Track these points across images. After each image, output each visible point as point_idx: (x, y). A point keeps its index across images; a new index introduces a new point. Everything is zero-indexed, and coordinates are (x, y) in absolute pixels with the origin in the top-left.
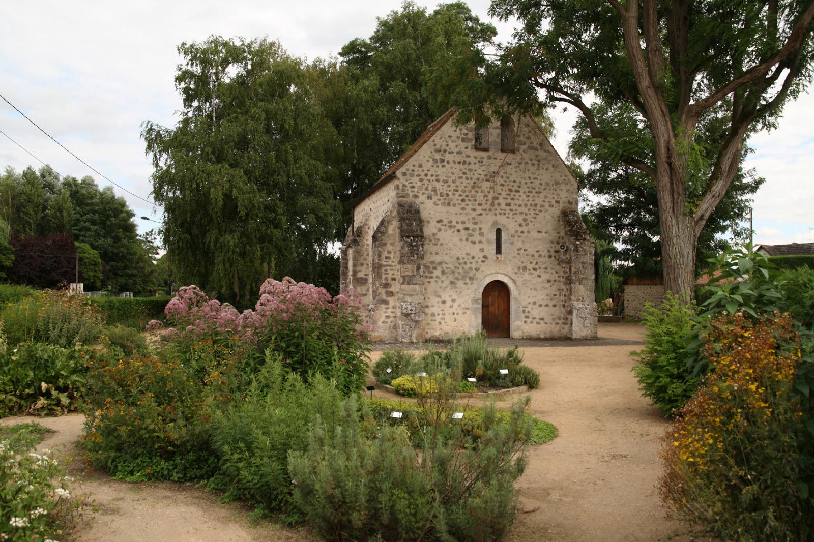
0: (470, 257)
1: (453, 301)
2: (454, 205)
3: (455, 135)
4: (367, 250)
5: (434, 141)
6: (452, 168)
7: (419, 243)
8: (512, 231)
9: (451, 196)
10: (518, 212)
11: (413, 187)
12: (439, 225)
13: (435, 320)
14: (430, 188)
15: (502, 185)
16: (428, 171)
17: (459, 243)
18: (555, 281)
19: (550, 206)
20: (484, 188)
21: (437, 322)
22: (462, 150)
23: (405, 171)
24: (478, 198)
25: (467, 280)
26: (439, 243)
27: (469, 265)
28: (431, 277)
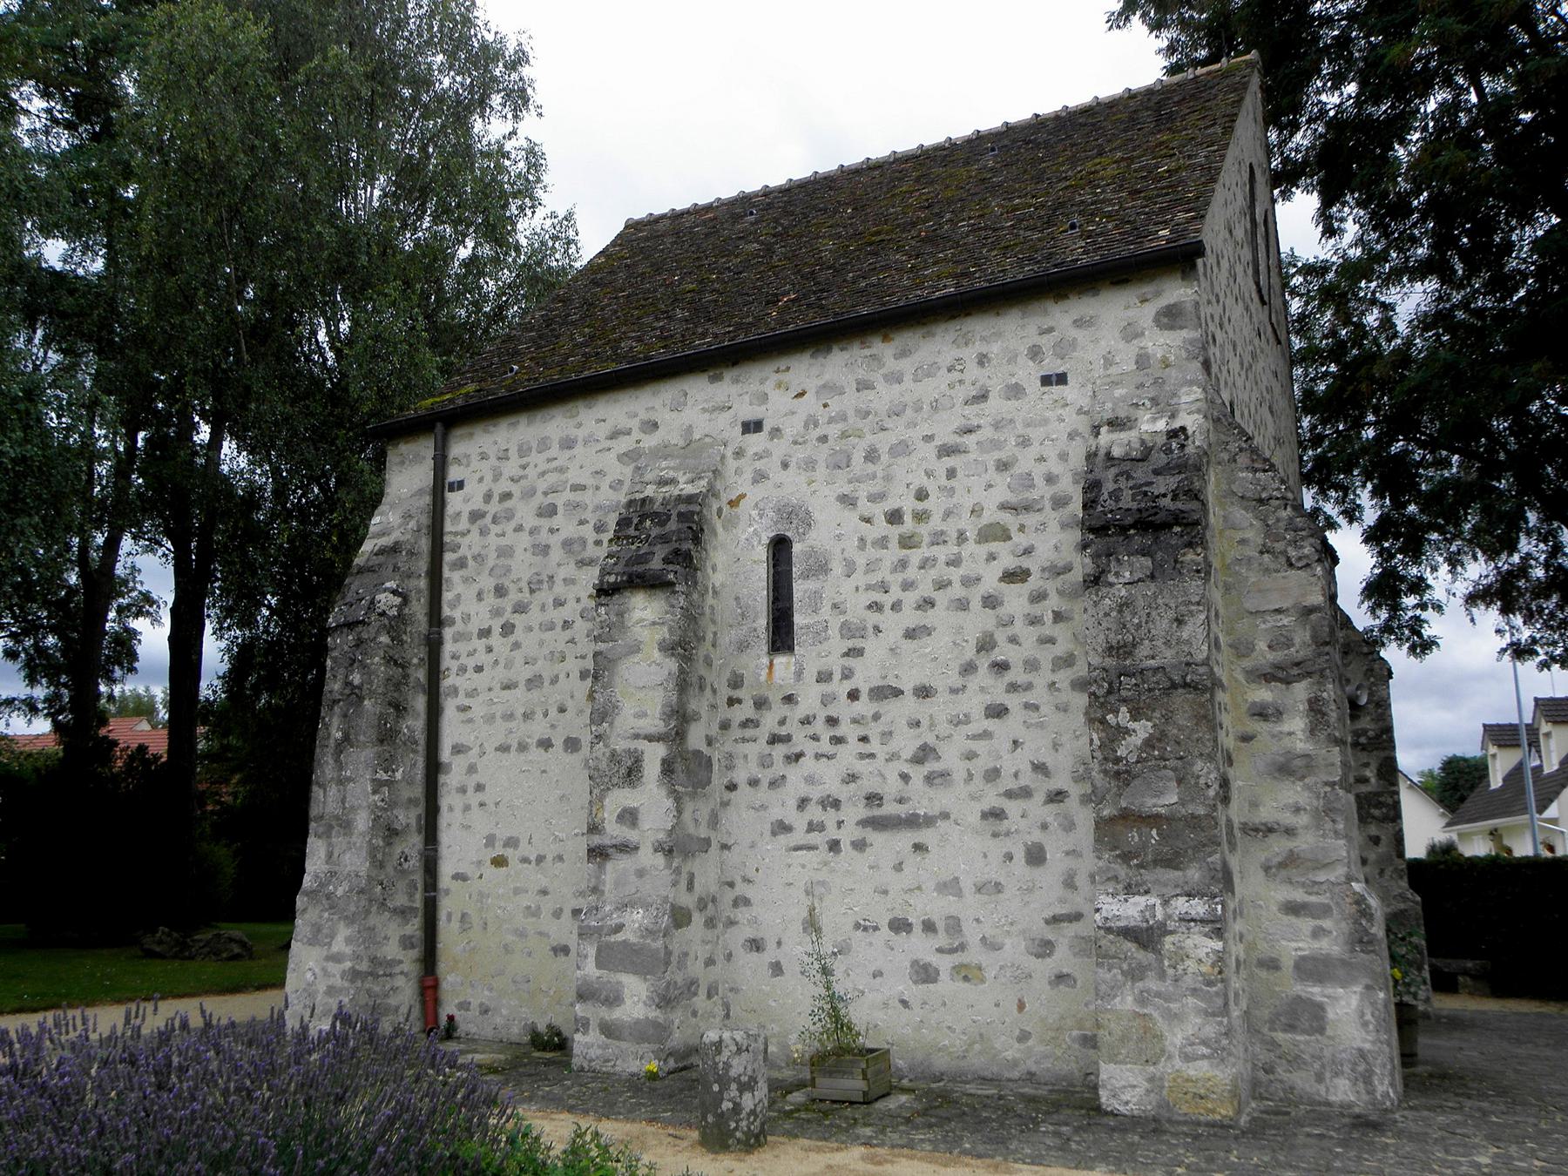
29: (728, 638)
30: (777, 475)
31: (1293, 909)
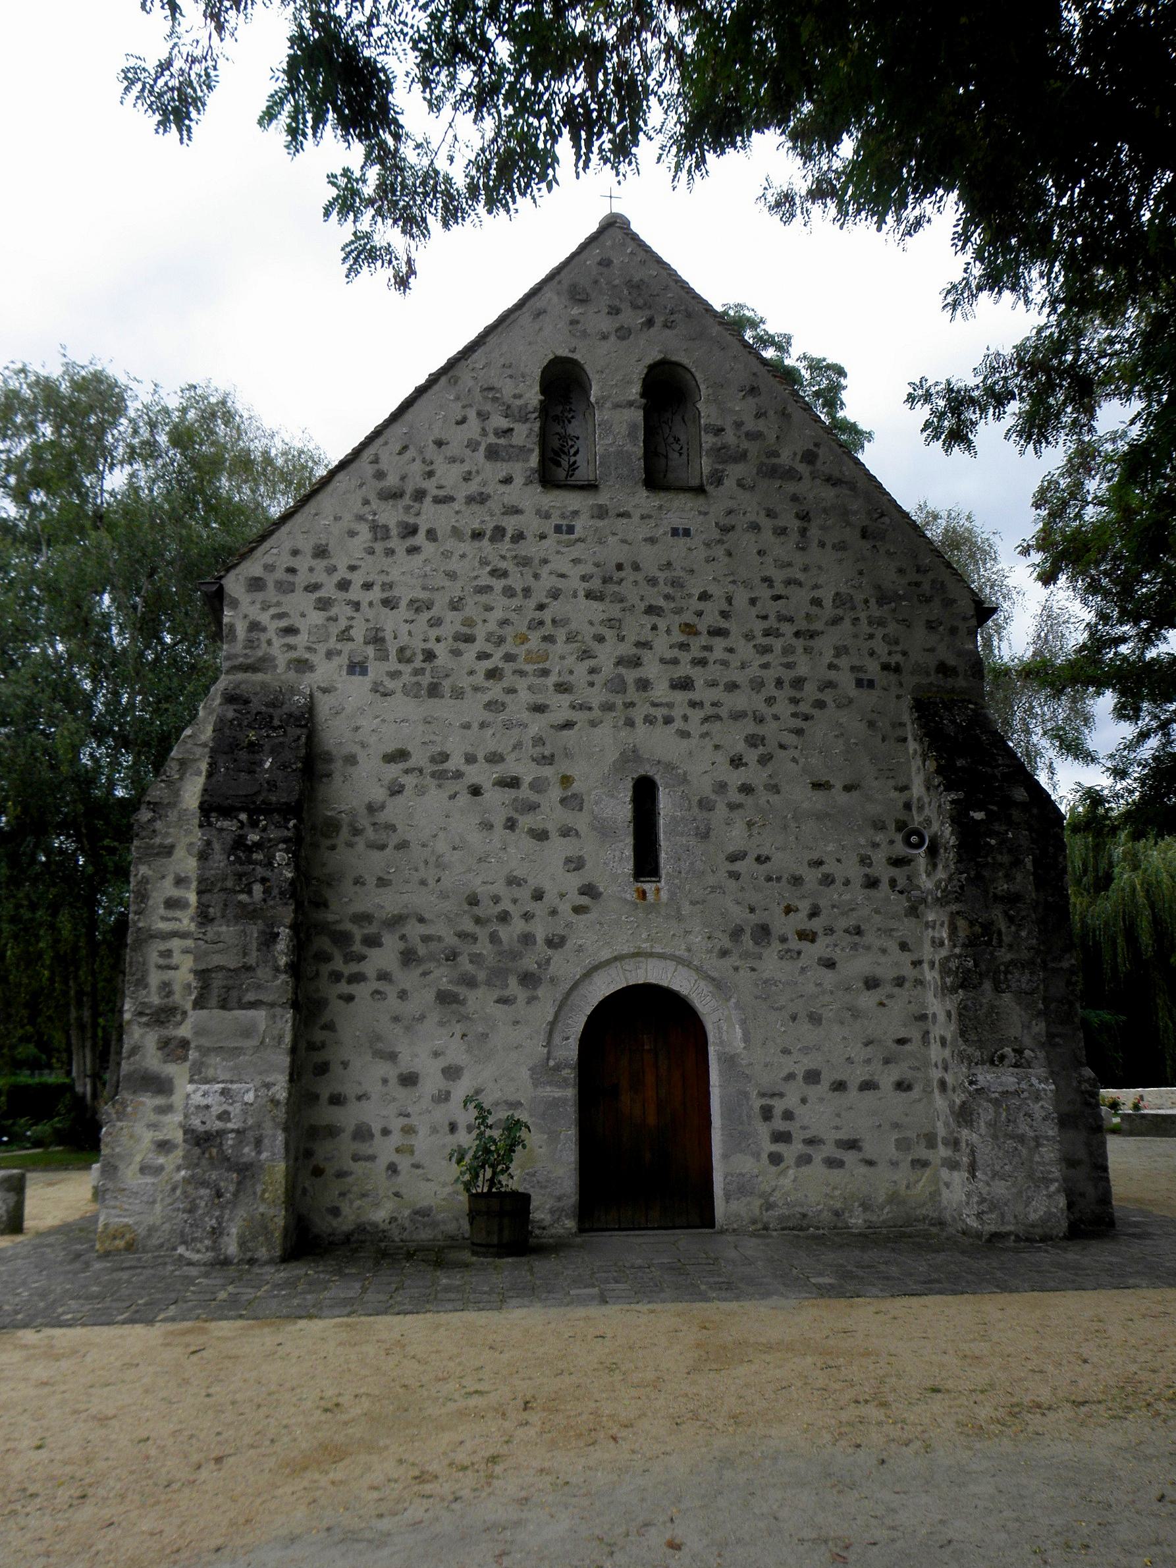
0: (524, 893)
1: (452, 1073)
2: (458, 694)
3: (458, 438)
5: (376, 461)
6: (447, 555)
8: (703, 786)
10: (723, 712)
11: (291, 631)
13: (372, 1158)
14: (358, 633)
15: (651, 610)
16: (352, 568)
17: (475, 838)
18: (900, 982)
19: (859, 683)
22: (488, 490)
25: (513, 987)
26: (394, 840)
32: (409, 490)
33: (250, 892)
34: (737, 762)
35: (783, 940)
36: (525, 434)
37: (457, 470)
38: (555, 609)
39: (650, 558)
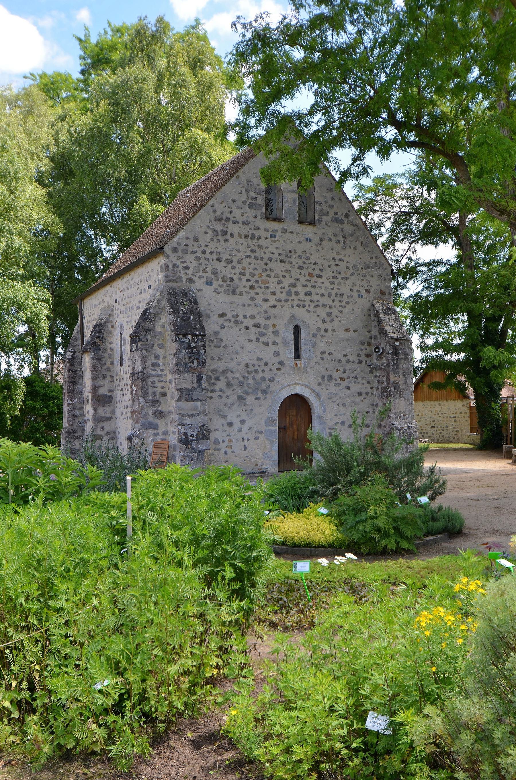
0: (262, 363)
1: (243, 422)
2: (241, 294)
3: (240, 199)
4: (111, 356)
5: (213, 206)
7: (200, 344)
9: (236, 281)
10: (320, 304)
11: (187, 268)
12: (221, 320)
13: (219, 450)
14: (209, 270)
15: (300, 268)
16: (206, 246)
18: (367, 394)
19: (359, 296)
20: (278, 271)
21: (223, 451)
22: (250, 220)
23: (175, 245)
24: (271, 285)
25: (260, 395)
26: (223, 344)
27: (260, 374)
28: (213, 391)
29: (115, 362)
30: (121, 316)
31: (173, 433)
32: (224, 218)
33: (193, 363)
34: (324, 321)
35: (336, 380)
36: (261, 200)
37: (239, 212)
38: (271, 265)
39: (300, 249)
